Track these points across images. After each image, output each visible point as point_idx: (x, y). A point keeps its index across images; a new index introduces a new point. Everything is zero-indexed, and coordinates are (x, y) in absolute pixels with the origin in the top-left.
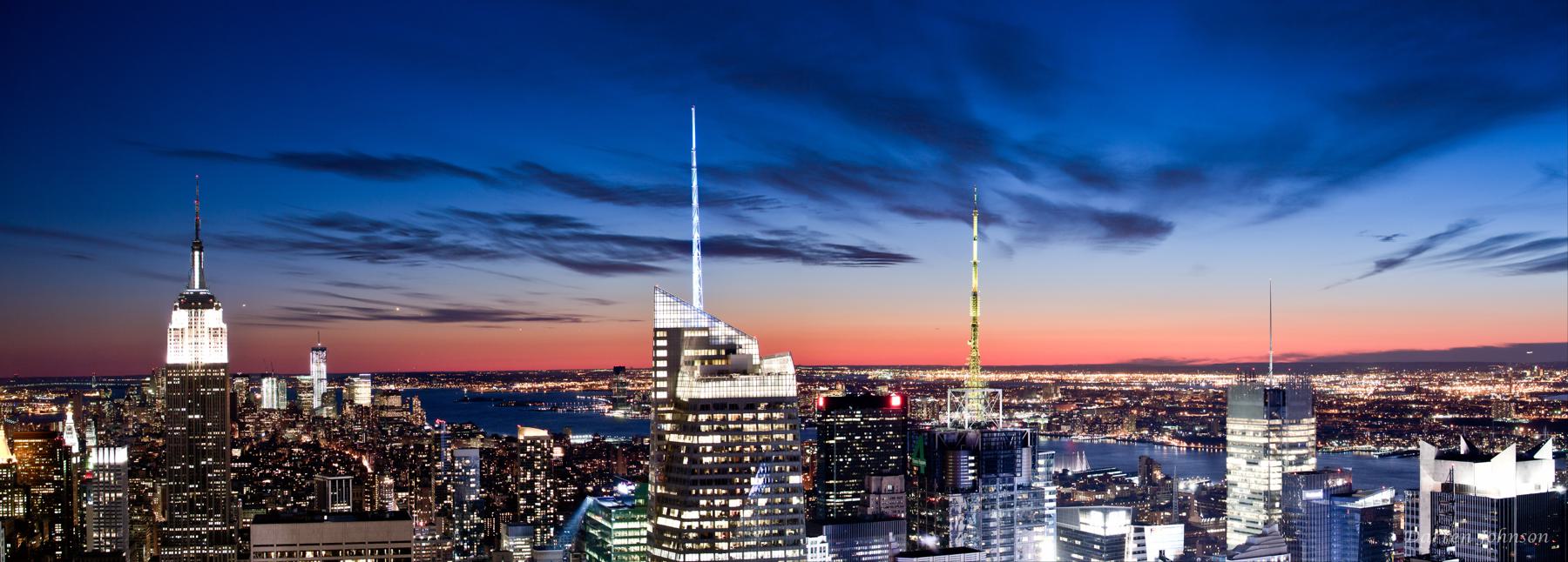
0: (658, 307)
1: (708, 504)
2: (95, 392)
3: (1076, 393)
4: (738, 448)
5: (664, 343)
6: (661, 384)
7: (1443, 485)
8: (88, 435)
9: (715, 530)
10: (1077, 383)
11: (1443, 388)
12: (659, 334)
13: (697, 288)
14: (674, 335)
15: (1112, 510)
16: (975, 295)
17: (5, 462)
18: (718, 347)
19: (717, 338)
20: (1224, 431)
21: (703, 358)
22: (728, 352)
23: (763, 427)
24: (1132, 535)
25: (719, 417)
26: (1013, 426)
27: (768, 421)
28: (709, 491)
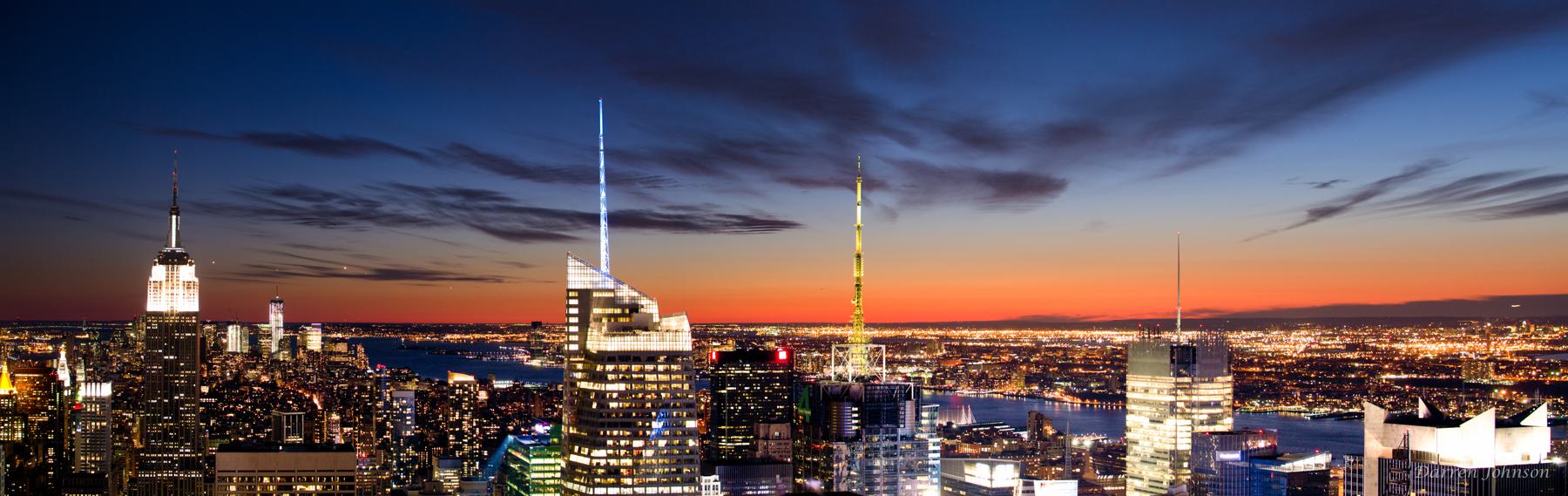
0: (570, 271)
1: (614, 444)
2: (85, 334)
3: (960, 349)
4: (640, 395)
5: (575, 302)
6: (572, 338)
7: (1394, 451)
8: (78, 371)
9: (620, 467)
10: (962, 339)
11: (1395, 346)
12: (571, 294)
13: (604, 255)
14: (585, 296)
15: (999, 463)
16: (859, 256)
17: (7, 393)
18: (623, 307)
19: (621, 298)
20: (1124, 388)
21: (609, 316)
22: (631, 312)
23: (663, 377)
24: (1021, 488)
25: (623, 367)
26: (896, 380)
27: (666, 372)
28: (615, 433)
